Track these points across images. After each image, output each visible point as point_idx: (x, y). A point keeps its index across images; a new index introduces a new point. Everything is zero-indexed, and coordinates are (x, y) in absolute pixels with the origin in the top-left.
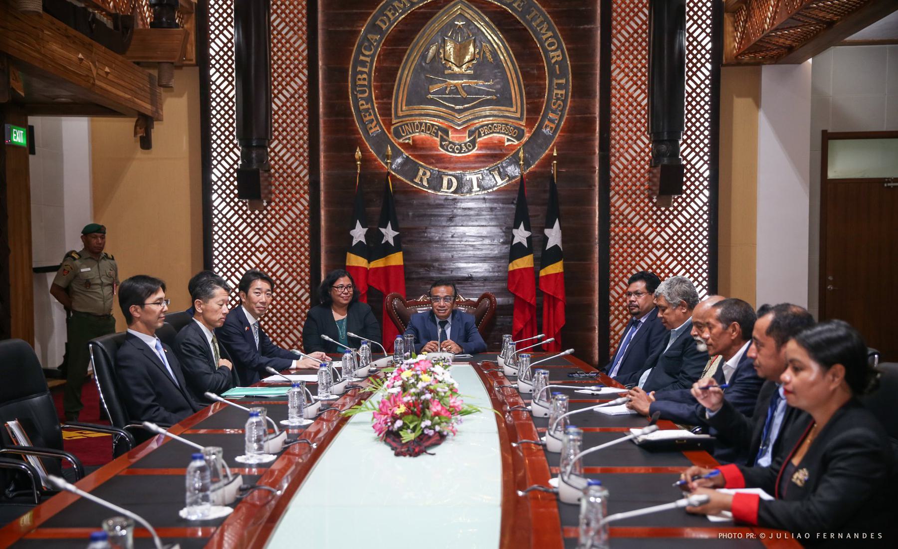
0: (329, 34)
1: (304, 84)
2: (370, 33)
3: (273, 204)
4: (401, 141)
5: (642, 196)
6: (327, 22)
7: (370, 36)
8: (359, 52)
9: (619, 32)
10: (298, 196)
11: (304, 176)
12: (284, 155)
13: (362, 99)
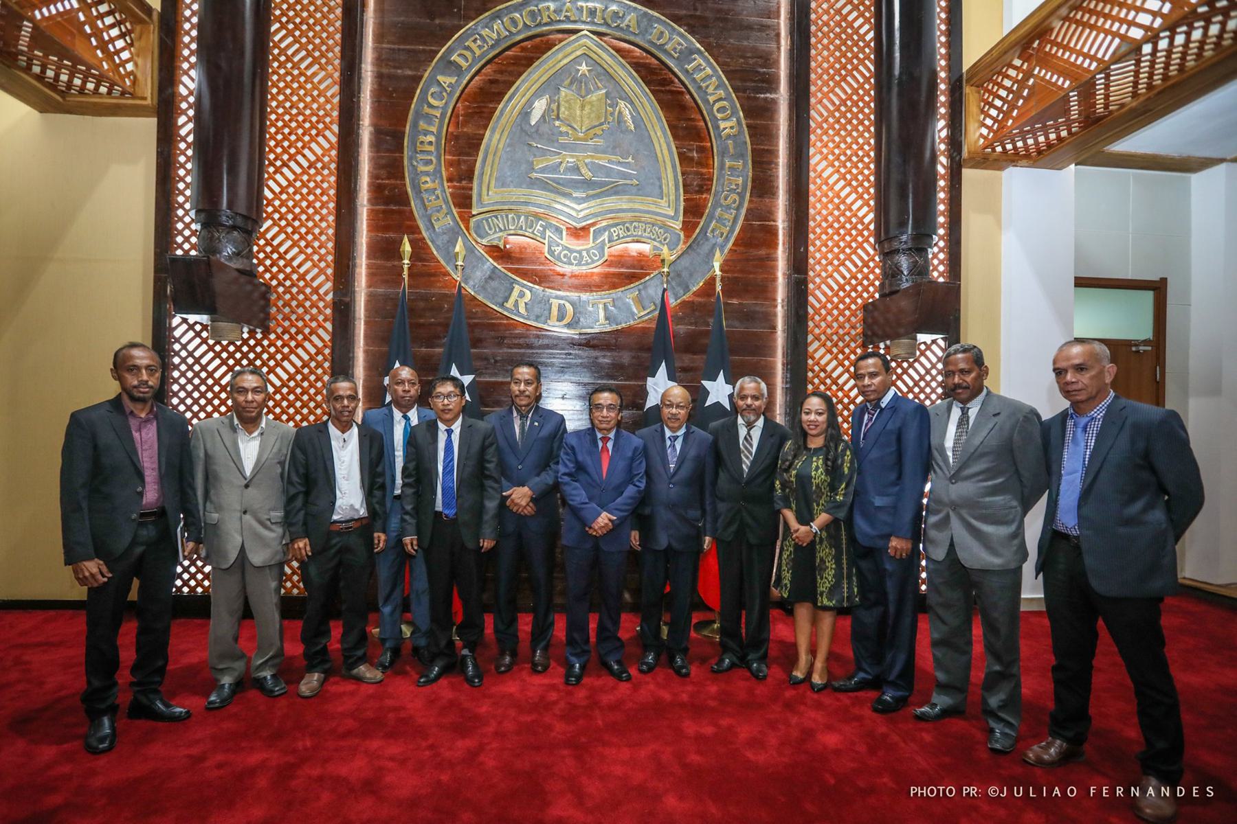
0: (379, 77)
1: (332, 147)
2: (443, 74)
3: (273, 336)
4: (484, 242)
5: (853, 345)
6: (379, 61)
7: (440, 78)
8: (423, 99)
9: (820, 102)
10: (314, 324)
11: (326, 293)
12: (293, 259)
13: (427, 174)
